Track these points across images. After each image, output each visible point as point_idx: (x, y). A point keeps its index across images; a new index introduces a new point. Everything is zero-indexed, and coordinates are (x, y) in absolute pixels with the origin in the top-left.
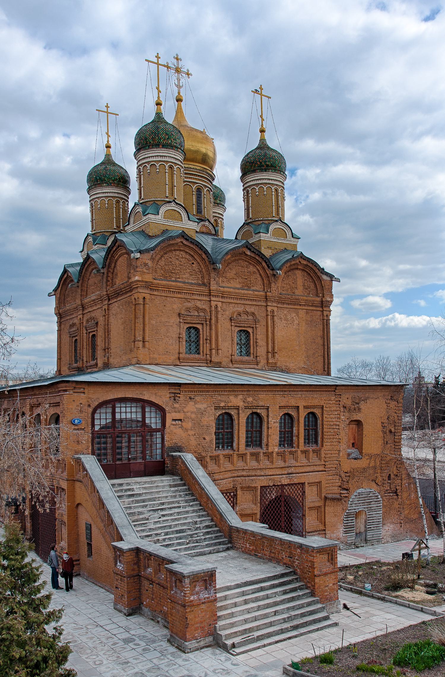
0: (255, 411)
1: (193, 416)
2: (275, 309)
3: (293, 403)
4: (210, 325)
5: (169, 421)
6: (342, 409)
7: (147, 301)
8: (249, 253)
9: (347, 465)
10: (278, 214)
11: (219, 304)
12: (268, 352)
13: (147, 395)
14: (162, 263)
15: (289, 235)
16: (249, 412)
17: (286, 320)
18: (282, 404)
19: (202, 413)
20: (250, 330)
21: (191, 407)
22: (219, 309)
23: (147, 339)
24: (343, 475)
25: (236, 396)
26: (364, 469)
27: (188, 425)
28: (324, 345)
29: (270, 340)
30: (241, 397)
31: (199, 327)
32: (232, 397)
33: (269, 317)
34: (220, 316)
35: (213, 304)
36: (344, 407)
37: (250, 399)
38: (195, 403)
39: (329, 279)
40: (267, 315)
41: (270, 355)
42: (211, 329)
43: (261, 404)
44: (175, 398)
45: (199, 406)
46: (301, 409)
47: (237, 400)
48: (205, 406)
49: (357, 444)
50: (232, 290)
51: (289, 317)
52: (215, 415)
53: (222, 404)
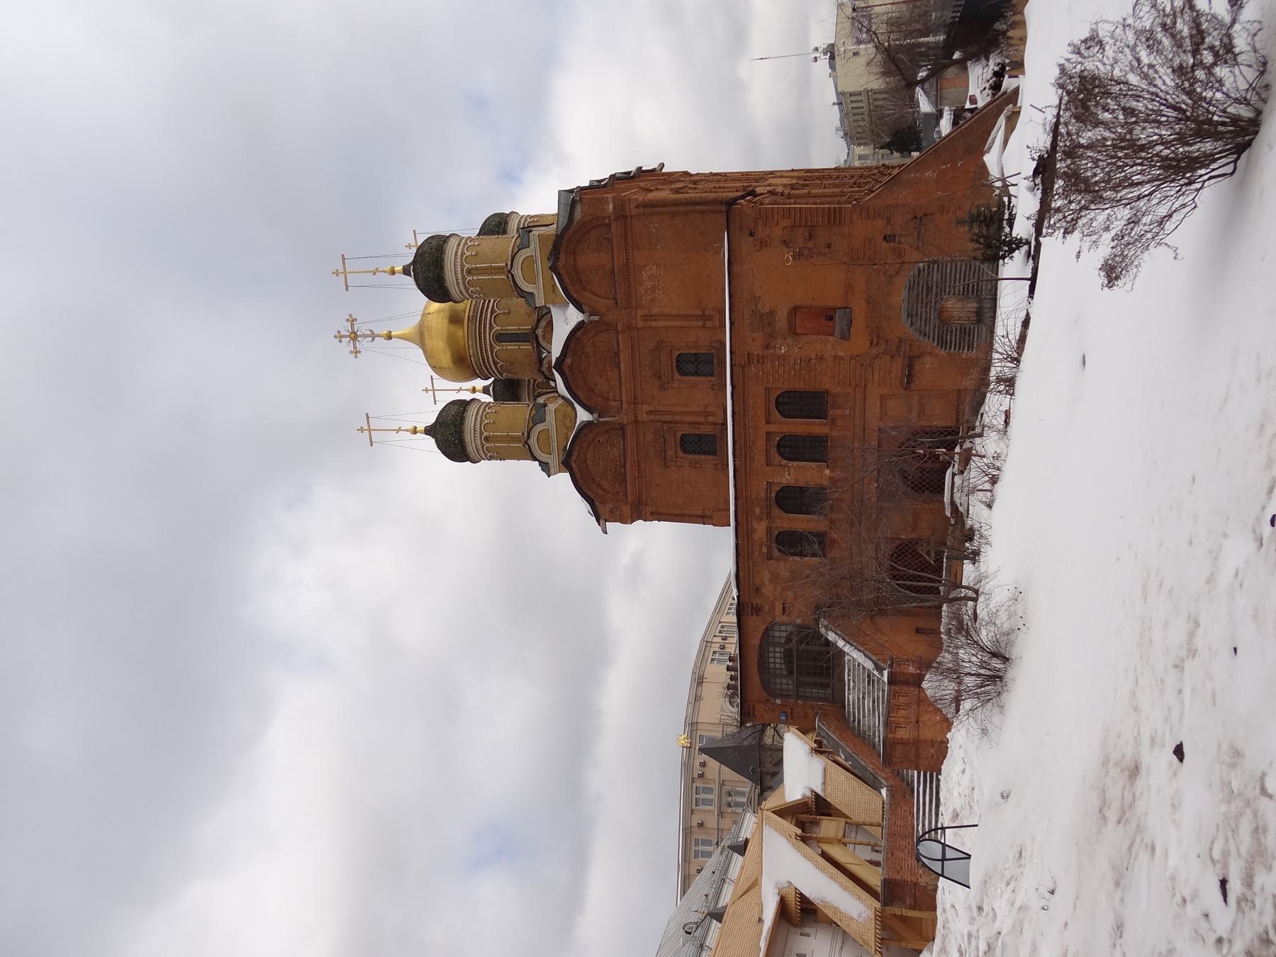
0: (773, 501)
1: (779, 589)
2: (640, 312)
3: (761, 443)
4: (675, 422)
5: (785, 618)
6: (771, 351)
7: (654, 509)
8: (569, 360)
9: (860, 341)
10: (499, 270)
11: (646, 408)
12: (704, 327)
13: (755, 641)
14: (605, 484)
15: (525, 253)
16: (776, 511)
17: (653, 289)
18: (763, 461)
19: (775, 578)
20: (676, 354)
21: (768, 590)
22: (651, 408)
23: (700, 513)
24: (874, 351)
25: (754, 530)
26: (868, 303)
27: (790, 594)
28: (686, 213)
29: (685, 323)
30: (755, 524)
31: (679, 436)
32: (756, 537)
33: (653, 324)
34: (662, 408)
35: (645, 418)
36: (767, 347)
37: (757, 510)
38: (763, 584)
39: (579, 208)
40: (650, 327)
41: (708, 324)
42: (680, 422)
43: (763, 495)
44: (757, 610)
45: (766, 580)
46: (771, 428)
47: (760, 530)
48: (766, 572)
49: (826, 317)
50: (623, 388)
51: (649, 284)
52: (778, 560)
53: (765, 550)
